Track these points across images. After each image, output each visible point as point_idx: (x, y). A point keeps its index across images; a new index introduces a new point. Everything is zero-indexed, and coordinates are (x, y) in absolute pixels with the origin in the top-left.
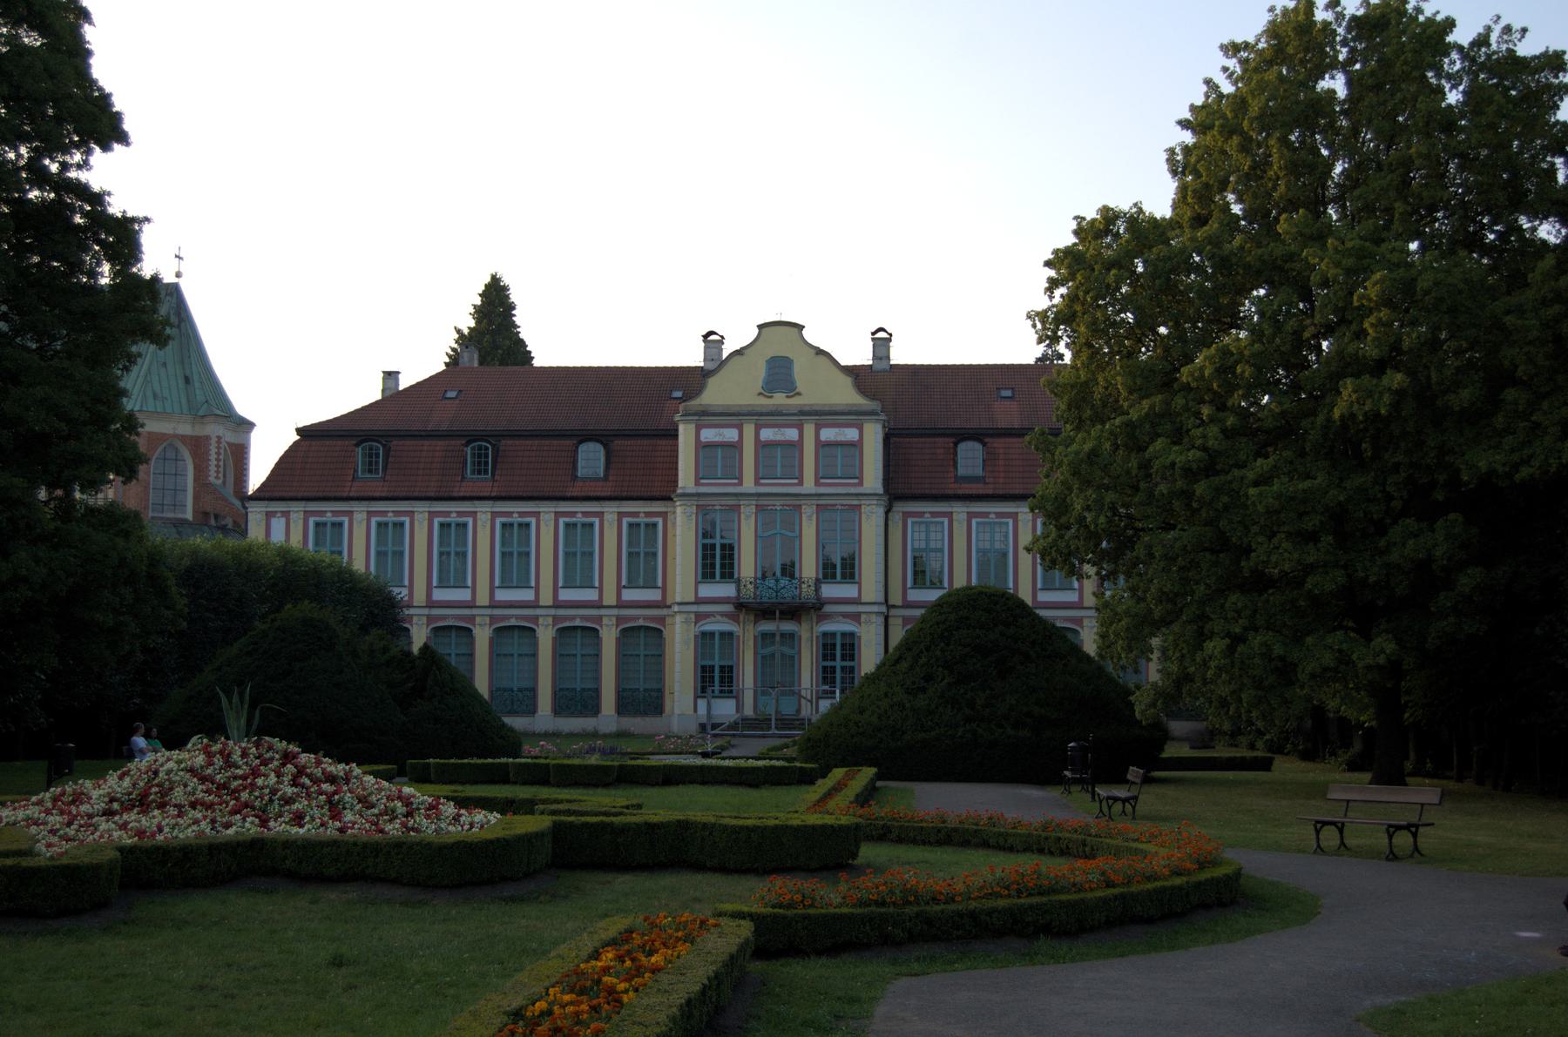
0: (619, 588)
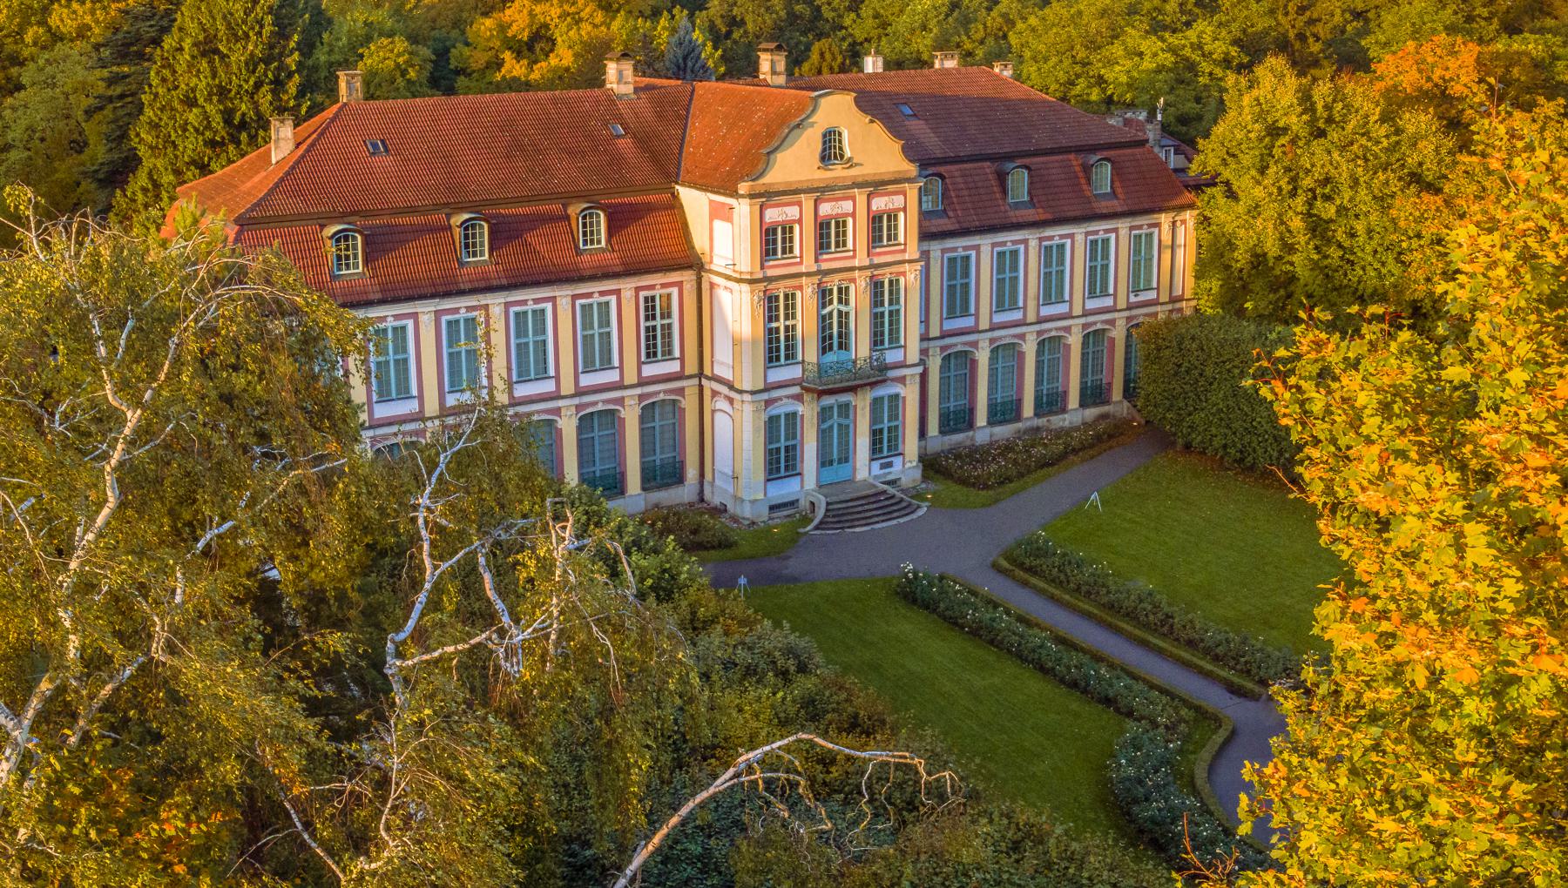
0: (640, 364)
